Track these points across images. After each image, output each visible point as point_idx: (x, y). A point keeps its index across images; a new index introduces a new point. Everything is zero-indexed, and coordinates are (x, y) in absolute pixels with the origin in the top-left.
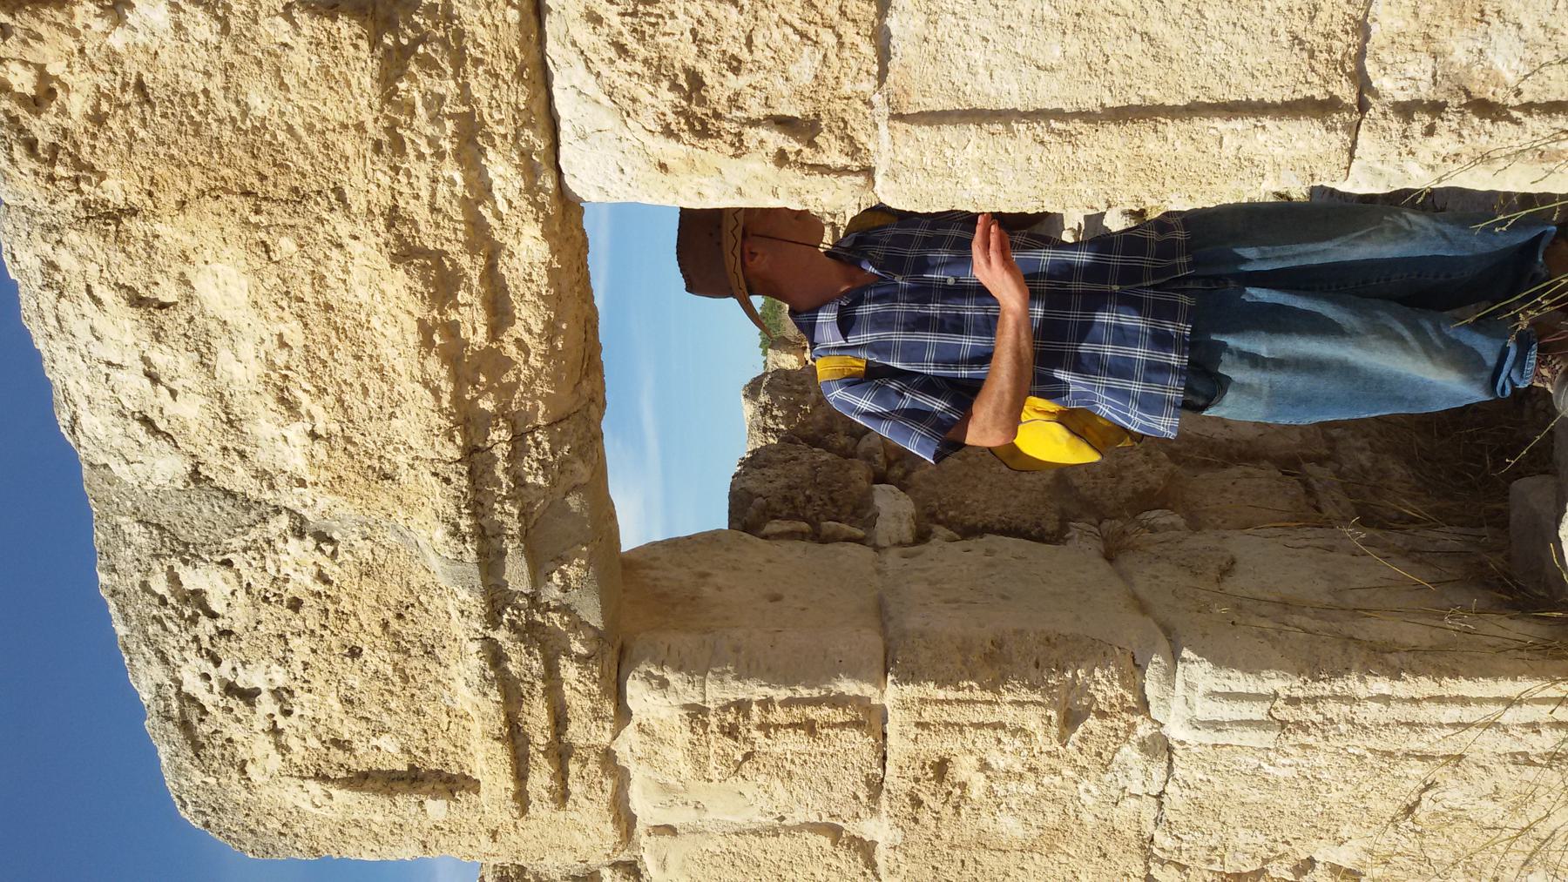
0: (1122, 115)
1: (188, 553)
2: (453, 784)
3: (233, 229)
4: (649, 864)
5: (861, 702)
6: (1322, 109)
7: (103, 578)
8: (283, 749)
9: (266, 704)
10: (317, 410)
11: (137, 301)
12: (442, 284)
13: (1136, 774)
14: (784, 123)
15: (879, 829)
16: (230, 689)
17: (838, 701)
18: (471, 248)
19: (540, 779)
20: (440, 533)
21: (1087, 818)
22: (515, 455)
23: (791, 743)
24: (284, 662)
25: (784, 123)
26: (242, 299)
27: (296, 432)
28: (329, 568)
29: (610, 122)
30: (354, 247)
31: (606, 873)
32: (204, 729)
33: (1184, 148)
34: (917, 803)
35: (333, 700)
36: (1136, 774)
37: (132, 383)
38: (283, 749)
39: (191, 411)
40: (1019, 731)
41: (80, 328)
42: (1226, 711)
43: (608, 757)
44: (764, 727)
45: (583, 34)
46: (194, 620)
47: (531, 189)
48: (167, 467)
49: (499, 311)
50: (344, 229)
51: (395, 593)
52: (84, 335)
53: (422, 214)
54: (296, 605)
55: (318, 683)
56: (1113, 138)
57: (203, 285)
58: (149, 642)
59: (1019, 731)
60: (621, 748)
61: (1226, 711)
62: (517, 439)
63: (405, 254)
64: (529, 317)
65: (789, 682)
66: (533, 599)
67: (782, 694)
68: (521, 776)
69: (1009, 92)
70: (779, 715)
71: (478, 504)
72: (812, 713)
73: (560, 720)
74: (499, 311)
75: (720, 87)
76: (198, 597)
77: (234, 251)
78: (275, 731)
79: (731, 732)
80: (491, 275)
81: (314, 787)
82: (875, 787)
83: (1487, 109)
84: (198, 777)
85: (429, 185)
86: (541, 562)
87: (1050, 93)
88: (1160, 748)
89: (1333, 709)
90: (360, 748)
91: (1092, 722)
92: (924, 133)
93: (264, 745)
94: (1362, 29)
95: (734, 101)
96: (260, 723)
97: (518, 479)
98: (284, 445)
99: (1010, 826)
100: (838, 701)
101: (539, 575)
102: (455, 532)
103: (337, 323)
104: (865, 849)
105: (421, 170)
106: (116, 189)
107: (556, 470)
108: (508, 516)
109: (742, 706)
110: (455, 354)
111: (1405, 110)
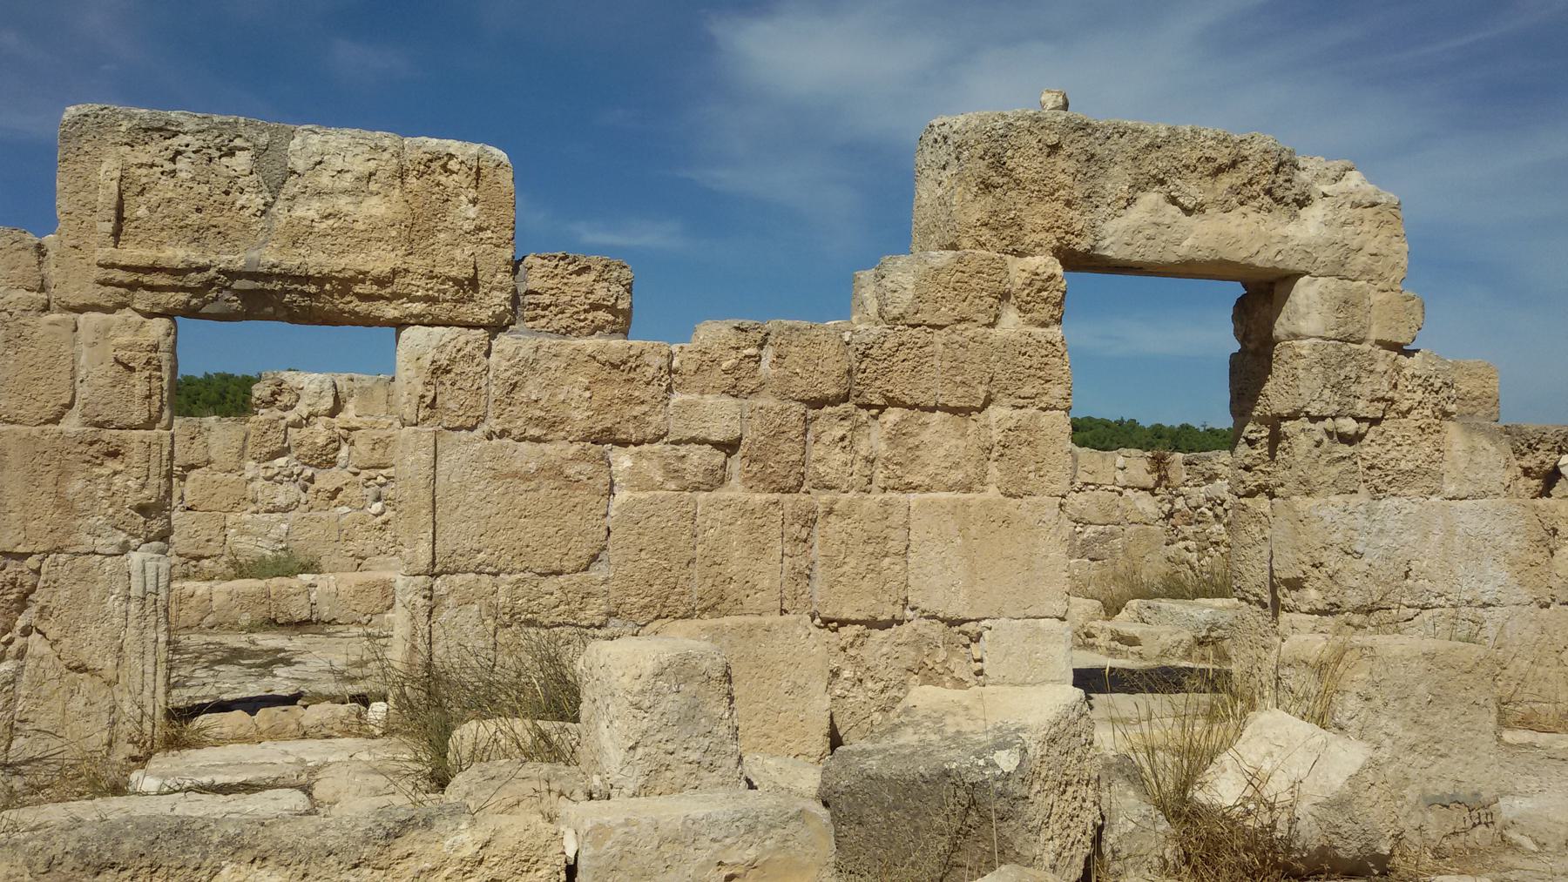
0: (434, 502)
1: (256, 158)
2: (117, 234)
3: (400, 217)
4: (55, 317)
5: (159, 419)
6: (434, 564)
7: (242, 119)
8: (141, 166)
9: (168, 166)
10: (323, 226)
11: (371, 175)
12: (381, 282)
13: (110, 540)
14: (435, 399)
15: (72, 424)
16: (178, 153)
17: (161, 410)
18: (393, 293)
19: (120, 275)
20: (273, 260)
21: (80, 521)
22: (303, 293)
23: (141, 389)
24: (193, 179)
25: (435, 399)
26: (373, 211)
27: (312, 214)
28: (247, 213)
29: (434, 343)
30: (393, 255)
31: (44, 296)
32: (156, 136)
33: (422, 521)
34: (91, 444)
35: (169, 195)
36: (110, 540)
37: (339, 164)
38: (141, 166)
39: (325, 180)
40: (143, 486)
41: (358, 150)
42: (151, 574)
43: (123, 306)
44: (150, 377)
45: (462, 339)
46: (219, 149)
47: (412, 315)
48: (300, 165)
50: (400, 253)
51: (233, 235)
52: (356, 151)
53: (407, 280)
54: (227, 193)
55: (180, 190)
56: (428, 499)
57: (375, 200)
58: (208, 129)
59: (143, 486)
60: (127, 312)
61: (151, 574)
62: (309, 295)
63: (395, 272)
64: (363, 307)
65: (170, 389)
66: (227, 288)
67: (165, 385)
68: (125, 268)
69: (443, 467)
70: (155, 383)
71: (285, 276)
72: (156, 398)
75: (447, 379)
76: (231, 153)
77: (390, 214)
78: (152, 166)
79: (148, 363)
80: (382, 297)
81: (117, 174)
82: (101, 425)
85: (420, 287)
86: (243, 295)
87: (441, 479)
88: (124, 549)
89: (152, 619)
90: (140, 199)
91: (142, 519)
92: (432, 441)
93: (145, 159)
94: (455, 572)
95: (442, 383)
96: (158, 161)
97: (289, 292)
98: (308, 210)
99: (76, 485)
100: (161, 410)
101: (237, 292)
102: (274, 266)
103: (363, 241)
104: (56, 420)
105: (422, 283)
106: (412, 182)
107: (287, 307)
108: (276, 285)
109: (159, 368)
110: (354, 280)
111: (431, 589)
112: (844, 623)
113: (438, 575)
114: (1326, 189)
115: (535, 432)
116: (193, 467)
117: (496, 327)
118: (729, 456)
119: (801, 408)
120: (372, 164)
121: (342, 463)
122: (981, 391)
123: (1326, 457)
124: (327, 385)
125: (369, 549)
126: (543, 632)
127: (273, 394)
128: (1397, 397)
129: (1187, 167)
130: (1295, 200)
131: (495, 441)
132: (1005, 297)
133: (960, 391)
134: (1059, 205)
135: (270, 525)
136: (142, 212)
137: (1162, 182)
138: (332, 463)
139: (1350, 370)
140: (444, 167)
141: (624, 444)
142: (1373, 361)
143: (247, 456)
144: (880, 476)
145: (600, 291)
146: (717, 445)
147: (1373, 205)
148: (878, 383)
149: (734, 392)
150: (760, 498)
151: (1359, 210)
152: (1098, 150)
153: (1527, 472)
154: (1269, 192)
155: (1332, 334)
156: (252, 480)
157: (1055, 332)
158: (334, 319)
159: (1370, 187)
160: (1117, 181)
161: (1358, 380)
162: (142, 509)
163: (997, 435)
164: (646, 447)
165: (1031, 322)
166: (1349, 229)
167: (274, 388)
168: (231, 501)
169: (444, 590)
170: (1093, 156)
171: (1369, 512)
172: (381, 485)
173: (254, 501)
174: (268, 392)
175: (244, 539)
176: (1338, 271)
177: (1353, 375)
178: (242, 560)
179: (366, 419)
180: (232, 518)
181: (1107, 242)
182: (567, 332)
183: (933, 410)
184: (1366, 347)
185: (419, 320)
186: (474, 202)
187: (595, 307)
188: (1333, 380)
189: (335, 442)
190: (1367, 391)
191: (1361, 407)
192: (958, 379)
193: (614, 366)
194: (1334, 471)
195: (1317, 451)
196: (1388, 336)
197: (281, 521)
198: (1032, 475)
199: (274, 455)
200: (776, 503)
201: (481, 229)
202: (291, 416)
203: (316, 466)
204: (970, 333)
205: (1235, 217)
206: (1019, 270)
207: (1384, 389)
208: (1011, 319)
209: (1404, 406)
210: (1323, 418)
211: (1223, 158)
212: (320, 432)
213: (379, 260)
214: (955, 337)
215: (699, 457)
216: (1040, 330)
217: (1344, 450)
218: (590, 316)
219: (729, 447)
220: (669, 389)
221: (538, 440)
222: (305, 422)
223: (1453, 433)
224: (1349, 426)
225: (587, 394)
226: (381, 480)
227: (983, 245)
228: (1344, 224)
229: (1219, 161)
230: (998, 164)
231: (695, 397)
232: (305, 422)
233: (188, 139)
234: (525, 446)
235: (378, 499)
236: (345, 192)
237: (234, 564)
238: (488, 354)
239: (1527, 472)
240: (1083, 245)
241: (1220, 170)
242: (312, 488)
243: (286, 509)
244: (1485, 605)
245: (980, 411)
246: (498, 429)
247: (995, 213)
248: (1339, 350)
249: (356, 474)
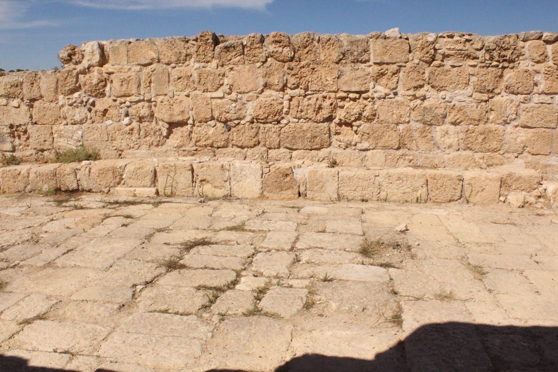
116: (34, 100)
121: (108, 94)
124: (96, 47)
125: (124, 146)
127: (70, 55)
135: (73, 132)
138: (103, 95)
143: (59, 93)
156: (62, 106)
167: (70, 51)
168: (53, 118)
172: (128, 107)
173: (65, 118)
174: (66, 54)
175: (62, 140)
178: (61, 151)
179: (116, 66)
180: (55, 128)
189: (104, 82)
197: (78, 129)
199: (72, 91)
202: (80, 67)
203: (96, 96)
212: (95, 76)
222: (87, 71)
226: (128, 104)
232: (87, 71)
235: (127, 115)
237: (57, 154)
242: (94, 109)
243: (81, 122)
249: (115, 101)
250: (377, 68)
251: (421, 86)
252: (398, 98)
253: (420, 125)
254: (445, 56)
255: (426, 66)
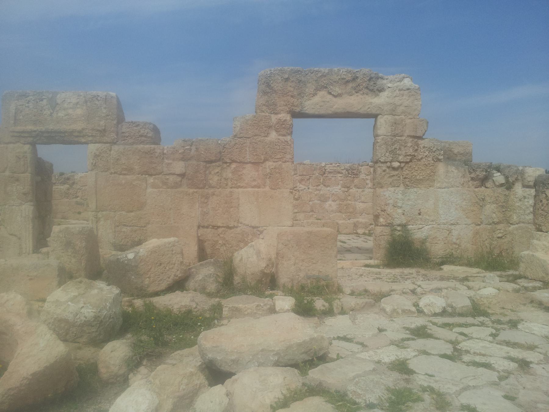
9: (27, 105)
11: (77, 103)
12: (80, 132)
15: (7, 173)
16: (29, 101)
39: (65, 105)
48: (59, 101)
49: (77, 136)
63: (83, 129)
73: (24, 137)
74: (77, 136)
76: (42, 100)
80: (80, 136)
83: (97, 222)
84: (16, 95)
104: (4, 171)
106: (89, 104)
109: (26, 158)
112: (219, 227)
113: (99, 212)
114: (389, 85)
115: (125, 172)
117: (114, 143)
118: (183, 178)
119: (205, 164)
120: (78, 100)
122: (262, 157)
123: (388, 175)
126: (128, 228)
128: (416, 154)
129: (335, 82)
130: (378, 90)
131: (113, 175)
132: (270, 127)
133: (255, 157)
134: (289, 98)
136: (21, 117)
137: (326, 87)
139: (396, 146)
140: (97, 99)
141: (151, 175)
142: (406, 143)
144: (230, 184)
145: (142, 132)
146: (178, 175)
147: (408, 89)
148: (229, 156)
149: (183, 159)
150: (191, 191)
151: (402, 92)
152: (303, 79)
153: (472, 179)
154: (367, 88)
155: (389, 134)
157: (289, 138)
158: (70, 143)
159: (411, 83)
160: (310, 88)
161: (400, 149)
162: (25, 194)
163: (268, 171)
164: (157, 176)
165: (280, 135)
166: (397, 98)
169: (100, 216)
170: (301, 81)
171: (403, 193)
176: (393, 112)
177: (398, 148)
181: (306, 108)
182: (133, 144)
183: (247, 163)
184: (403, 138)
185: (92, 142)
186: (105, 108)
187: (141, 136)
188: (390, 150)
190: (404, 152)
191: (401, 158)
192: (255, 154)
193: (146, 153)
194: (391, 180)
195: (384, 173)
196: (412, 134)
198: (280, 183)
200: (196, 192)
201: (108, 116)
204: (259, 139)
205: (352, 97)
206: (274, 118)
207: (411, 151)
208: (273, 135)
209: (420, 157)
210: (386, 162)
211: (349, 77)
213: (78, 126)
214: (254, 141)
215: (172, 178)
216: (284, 137)
217: (396, 173)
218: (140, 139)
219: (183, 175)
220: (163, 159)
221: (125, 174)
223: (441, 168)
224: (396, 164)
225: (139, 161)
227: (263, 112)
228: (396, 96)
229: (347, 79)
230: (268, 86)
231: (170, 161)
233: (31, 97)
234: (121, 176)
236: (71, 108)
238: (110, 150)
239: (472, 179)
240: (298, 110)
241: (348, 82)
244: (452, 224)
245: (262, 163)
246: (113, 172)
247: (267, 101)
248: (392, 139)
250: (300, 177)
251: (319, 185)
252: (310, 190)
253: (319, 202)
254: (330, 173)
255: (321, 176)
